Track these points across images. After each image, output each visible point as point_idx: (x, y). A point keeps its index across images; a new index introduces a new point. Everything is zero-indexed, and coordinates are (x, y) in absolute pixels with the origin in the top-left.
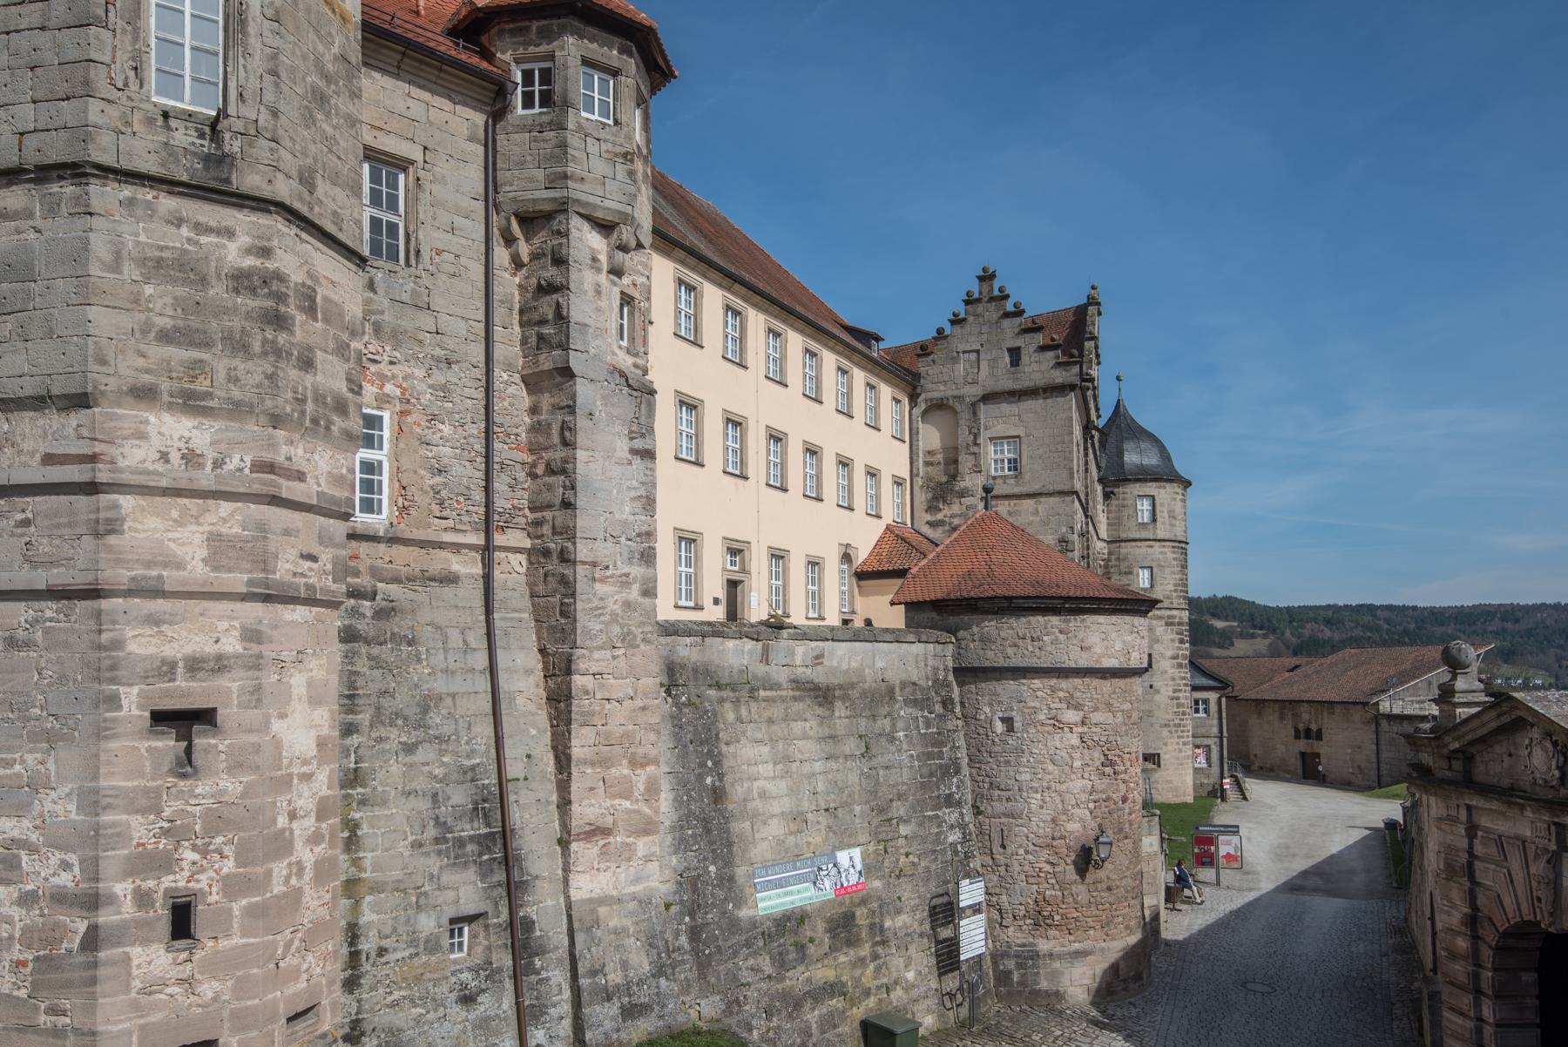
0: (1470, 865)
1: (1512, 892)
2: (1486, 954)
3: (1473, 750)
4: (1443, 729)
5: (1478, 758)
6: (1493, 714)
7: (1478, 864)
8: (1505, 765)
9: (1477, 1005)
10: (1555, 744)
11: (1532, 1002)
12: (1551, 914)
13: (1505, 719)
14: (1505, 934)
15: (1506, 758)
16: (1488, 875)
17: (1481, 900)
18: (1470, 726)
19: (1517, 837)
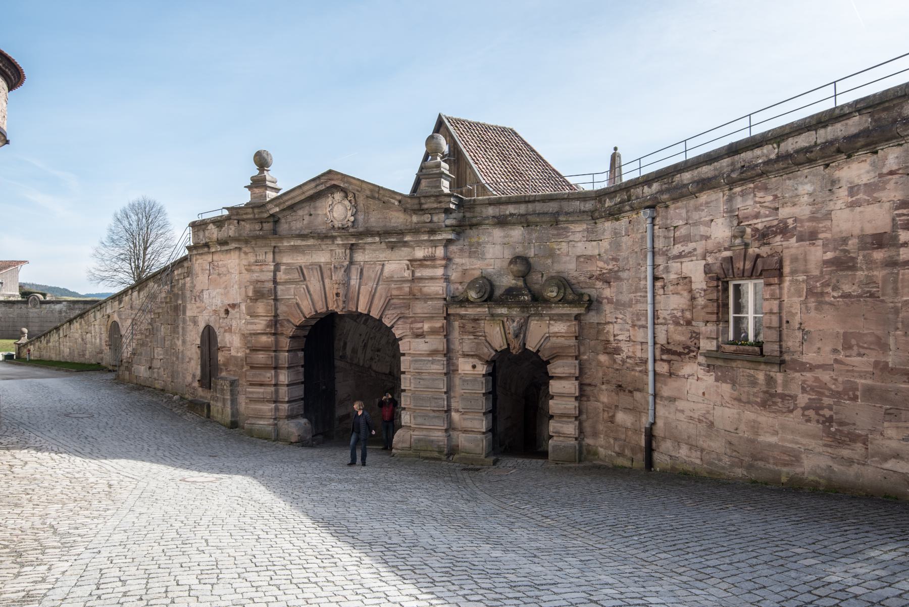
0: (275, 287)
1: (307, 299)
2: (285, 343)
3: (280, 216)
4: (256, 206)
5: (283, 221)
6: (313, 185)
7: (279, 288)
8: (305, 222)
9: (276, 376)
10: (350, 201)
11: (302, 370)
12: (344, 302)
13: (322, 187)
14: (299, 327)
15: (307, 218)
16: (287, 293)
17: (282, 308)
18: (292, 195)
19: (312, 264)
